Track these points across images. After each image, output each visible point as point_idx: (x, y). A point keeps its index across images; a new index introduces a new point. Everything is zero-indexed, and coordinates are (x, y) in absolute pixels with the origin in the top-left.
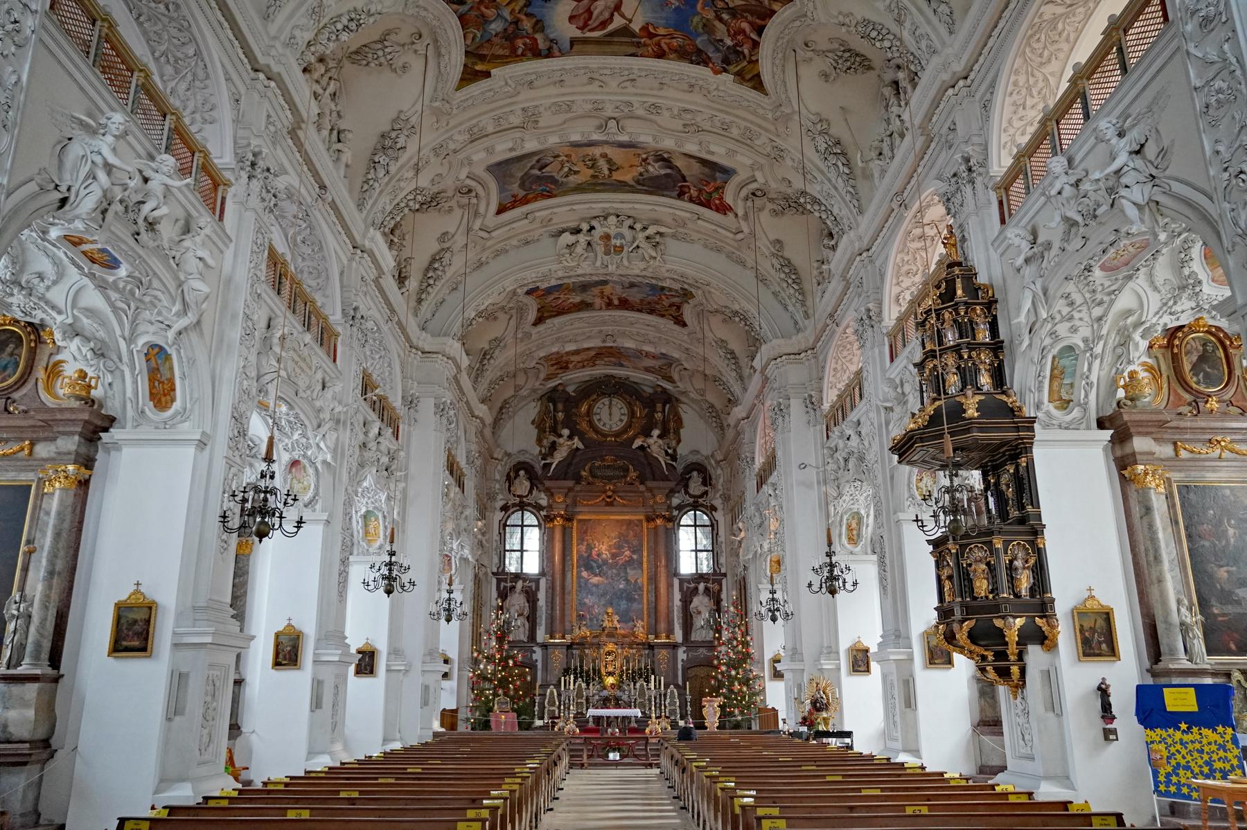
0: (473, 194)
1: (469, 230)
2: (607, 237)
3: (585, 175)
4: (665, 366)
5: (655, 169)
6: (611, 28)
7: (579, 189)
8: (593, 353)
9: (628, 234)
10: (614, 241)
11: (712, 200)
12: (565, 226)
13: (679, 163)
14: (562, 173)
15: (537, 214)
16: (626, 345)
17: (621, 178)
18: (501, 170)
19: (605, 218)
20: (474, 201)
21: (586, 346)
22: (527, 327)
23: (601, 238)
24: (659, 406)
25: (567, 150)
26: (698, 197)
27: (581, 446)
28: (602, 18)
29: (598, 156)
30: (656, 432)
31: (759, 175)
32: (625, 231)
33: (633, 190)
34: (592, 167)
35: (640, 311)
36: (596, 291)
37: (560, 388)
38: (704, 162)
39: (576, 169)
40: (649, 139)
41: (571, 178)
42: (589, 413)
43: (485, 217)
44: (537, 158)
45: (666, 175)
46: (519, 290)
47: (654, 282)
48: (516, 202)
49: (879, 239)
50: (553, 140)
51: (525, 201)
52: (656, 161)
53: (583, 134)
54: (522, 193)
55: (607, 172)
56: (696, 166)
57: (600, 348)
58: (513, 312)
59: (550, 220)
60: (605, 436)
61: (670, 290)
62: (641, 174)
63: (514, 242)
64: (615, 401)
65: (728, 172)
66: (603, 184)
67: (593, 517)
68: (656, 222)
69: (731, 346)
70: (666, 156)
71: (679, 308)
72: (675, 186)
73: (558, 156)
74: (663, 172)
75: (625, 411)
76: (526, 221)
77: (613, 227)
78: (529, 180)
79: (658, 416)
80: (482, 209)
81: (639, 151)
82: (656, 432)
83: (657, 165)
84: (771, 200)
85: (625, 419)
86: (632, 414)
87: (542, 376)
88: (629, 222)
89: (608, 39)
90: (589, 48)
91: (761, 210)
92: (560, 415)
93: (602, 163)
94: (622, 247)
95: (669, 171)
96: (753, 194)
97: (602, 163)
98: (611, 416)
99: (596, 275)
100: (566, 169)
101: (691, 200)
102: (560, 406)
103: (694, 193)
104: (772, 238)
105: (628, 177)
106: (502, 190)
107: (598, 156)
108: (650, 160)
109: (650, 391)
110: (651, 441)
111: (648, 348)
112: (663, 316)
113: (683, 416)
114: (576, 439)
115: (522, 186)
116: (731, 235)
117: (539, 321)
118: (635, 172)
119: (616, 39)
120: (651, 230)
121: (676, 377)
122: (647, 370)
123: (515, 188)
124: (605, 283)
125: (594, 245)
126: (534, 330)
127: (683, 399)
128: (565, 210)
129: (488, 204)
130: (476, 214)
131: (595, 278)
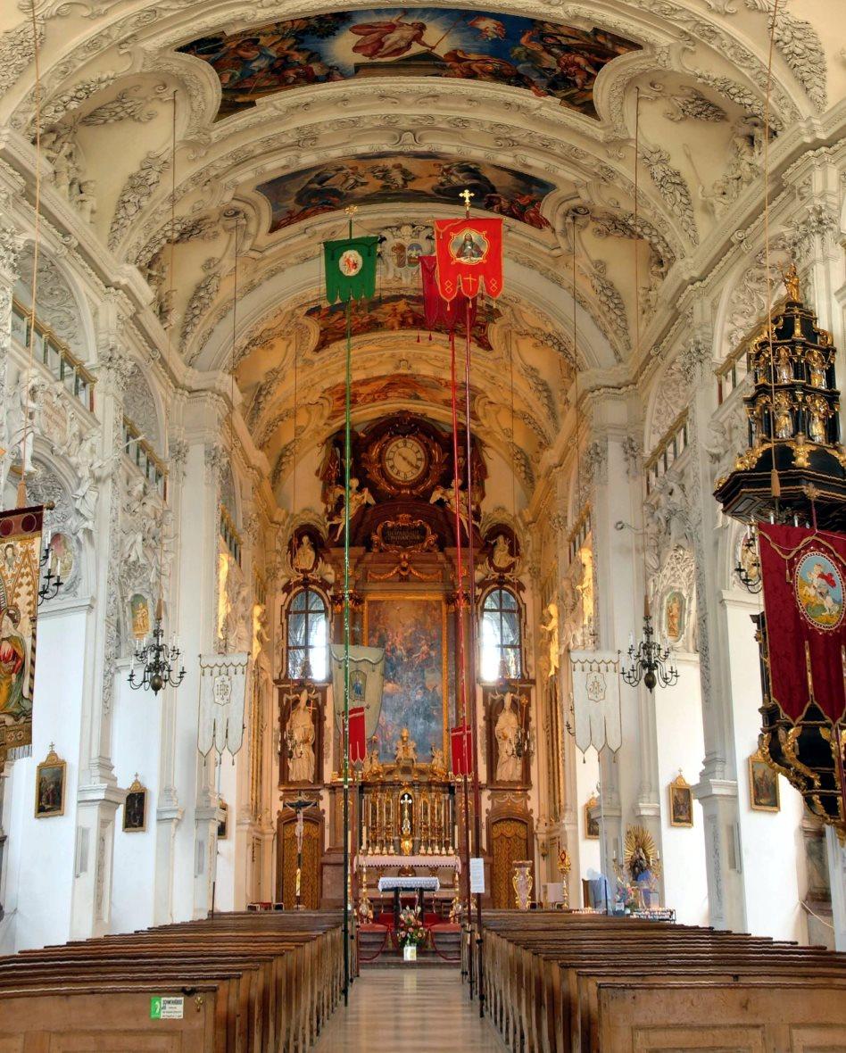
0: (242, 215)
3: (375, 185)
6: (407, 54)
7: (367, 200)
13: (489, 174)
15: (318, 228)
18: (273, 188)
19: (398, 228)
20: (244, 222)
25: (352, 163)
28: (396, 47)
31: (582, 193)
34: (383, 178)
38: (518, 175)
39: (363, 180)
40: (453, 150)
41: (358, 190)
43: (256, 236)
48: (292, 218)
49: (715, 272)
50: (336, 153)
51: (302, 216)
52: (461, 172)
54: (299, 208)
55: (400, 182)
62: (442, 184)
65: (546, 187)
66: (396, 194)
67: (387, 597)
70: (472, 167)
76: (305, 236)
78: (305, 194)
83: (461, 175)
84: (594, 219)
89: (405, 63)
90: (379, 71)
91: (585, 227)
95: (475, 182)
96: (575, 211)
100: (351, 181)
105: (425, 186)
106: (275, 207)
107: (390, 167)
108: (454, 170)
115: (299, 201)
118: (434, 182)
119: (413, 63)
123: (291, 204)
129: (259, 224)
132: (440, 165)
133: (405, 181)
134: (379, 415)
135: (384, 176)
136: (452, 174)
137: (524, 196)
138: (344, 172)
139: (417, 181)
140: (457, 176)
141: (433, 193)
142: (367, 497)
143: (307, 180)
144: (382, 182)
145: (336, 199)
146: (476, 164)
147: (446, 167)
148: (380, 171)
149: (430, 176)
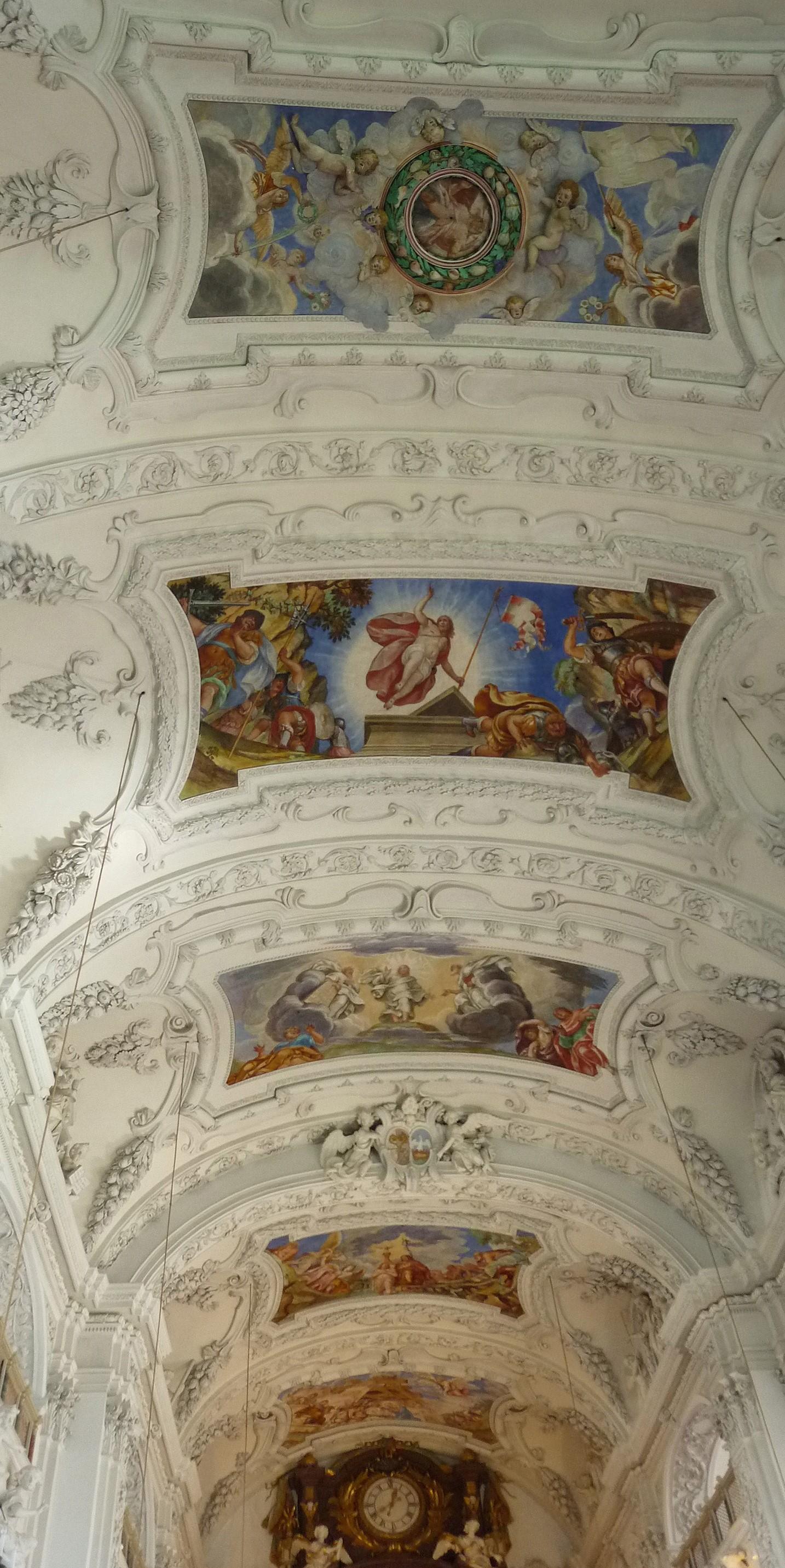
1: (182, 1106)
2: (401, 1137)
4: (479, 1406)
5: (485, 998)
7: (361, 1044)
8: (364, 1390)
9: (435, 1131)
10: (412, 1144)
11: (571, 1051)
12: (333, 1120)
13: (524, 978)
14: (335, 1007)
15: (293, 1090)
16: (420, 1369)
17: (427, 1020)
19: (399, 1106)
21: (354, 1372)
22: (265, 1325)
23: (393, 1138)
24: (470, 1486)
25: (346, 959)
26: (551, 1045)
27: (347, 1559)
29: (394, 972)
30: (472, 1526)
32: (429, 1126)
33: (448, 1046)
34: (385, 996)
35: (445, 1292)
36: (377, 1252)
37: (310, 1462)
39: (357, 1000)
41: (350, 1020)
42: (357, 1503)
43: (209, 1086)
44: (297, 971)
45: (503, 1008)
46: (257, 1237)
47: (474, 1225)
52: (485, 980)
53: (373, 920)
54: (270, 1045)
55: (406, 1008)
56: (550, 978)
57: (376, 1379)
58: (245, 1292)
59: (310, 1107)
60: (385, 1542)
61: (500, 1238)
63: (253, 1147)
64: (397, 1483)
66: (399, 1034)
68: (479, 1110)
69: (596, 1343)
70: (502, 966)
71: (511, 1276)
72: (513, 1030)
73: (329, 971)
74: (495, 1001)
75: (414, 1498)
76: (275, 1103)
77: (411, 1119)
79: (471, 1500)
80: (206, 1068)
81: (461, 960)
82: (472, 1526)
83: (486, 987)
85: (416, 1511)
86: (426, 1502)
87: (283, 1435)
88: (435, 1112)
89: (425, 719)
92: (310, 1507)
93: (400, 991)
94: (426, 1153)
95: (505, 998)
97: (400, 991)
98: (391, 1508)
99: (382, 1213)
100: (342, 1001)
101: (539, 1057)
102: (310, 1492)
103: (544, 1038)
104: (673, 1105)
106: (240, 1034)
108: (476, 980)
109: (451, 1462)
110: (465, 1541)
111: (455, 1371)
112: (482, 1299)
113: (511, 1503)
114: (340, 1543)
116: (604, 1114)
117: (285, 1313)
120: (473, 1123)
121: (498, 1428)
122: (451, 1421)
124: (392, 1232)
125: (383, 1152)
126: (275, 1332)
127: (506, 1471)
128: (334, 1089)
129: (216, 1060)
130: (196, 1075)
131: (379, 1222)
132: (459, 967)
133: (412, 1003)
134: (351, 1446)
135: (386, 991)
136: (474, 986)
137: (570, 1013)
138: (334, 978)
139: (428, 1002)
140: (481, 990)
141: (445, 1029)
142: (340, 1552)
143: (286, 984)
144: (380, 1007)
145: (320, 1036)
146: (506, 958)
147: (467, 970)
148: (380, 983)
149: (445, 994)
